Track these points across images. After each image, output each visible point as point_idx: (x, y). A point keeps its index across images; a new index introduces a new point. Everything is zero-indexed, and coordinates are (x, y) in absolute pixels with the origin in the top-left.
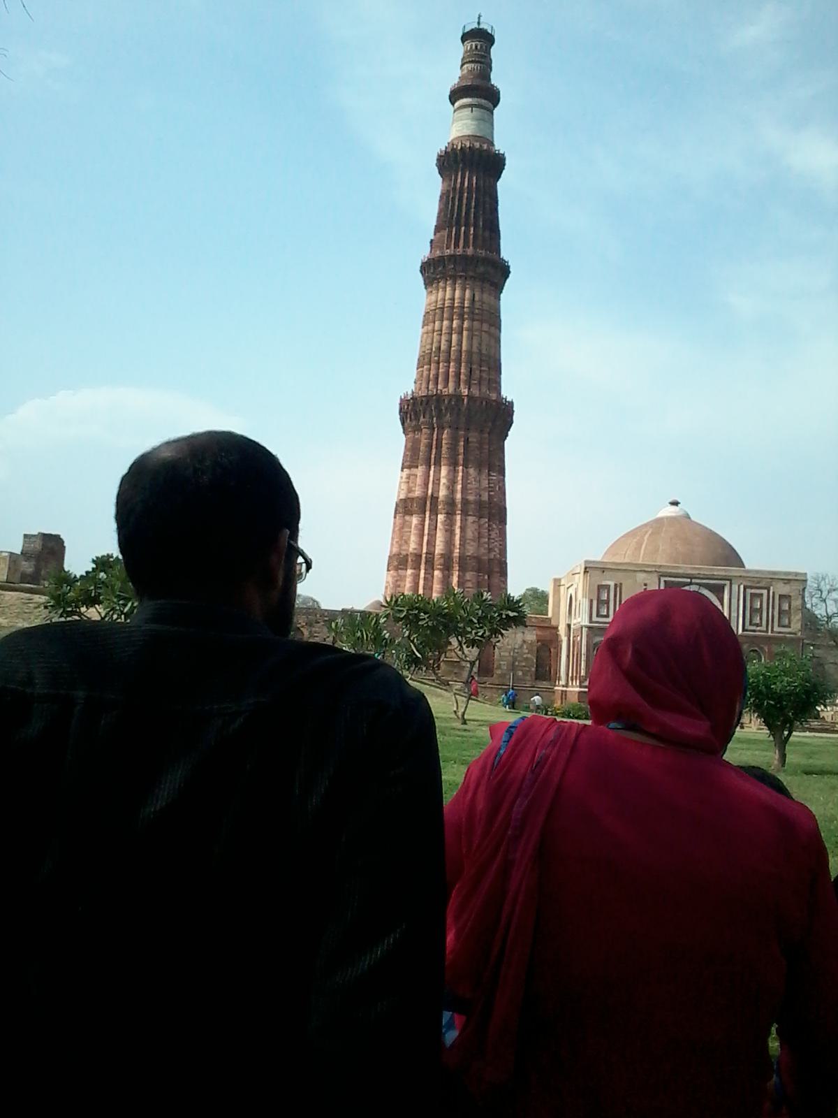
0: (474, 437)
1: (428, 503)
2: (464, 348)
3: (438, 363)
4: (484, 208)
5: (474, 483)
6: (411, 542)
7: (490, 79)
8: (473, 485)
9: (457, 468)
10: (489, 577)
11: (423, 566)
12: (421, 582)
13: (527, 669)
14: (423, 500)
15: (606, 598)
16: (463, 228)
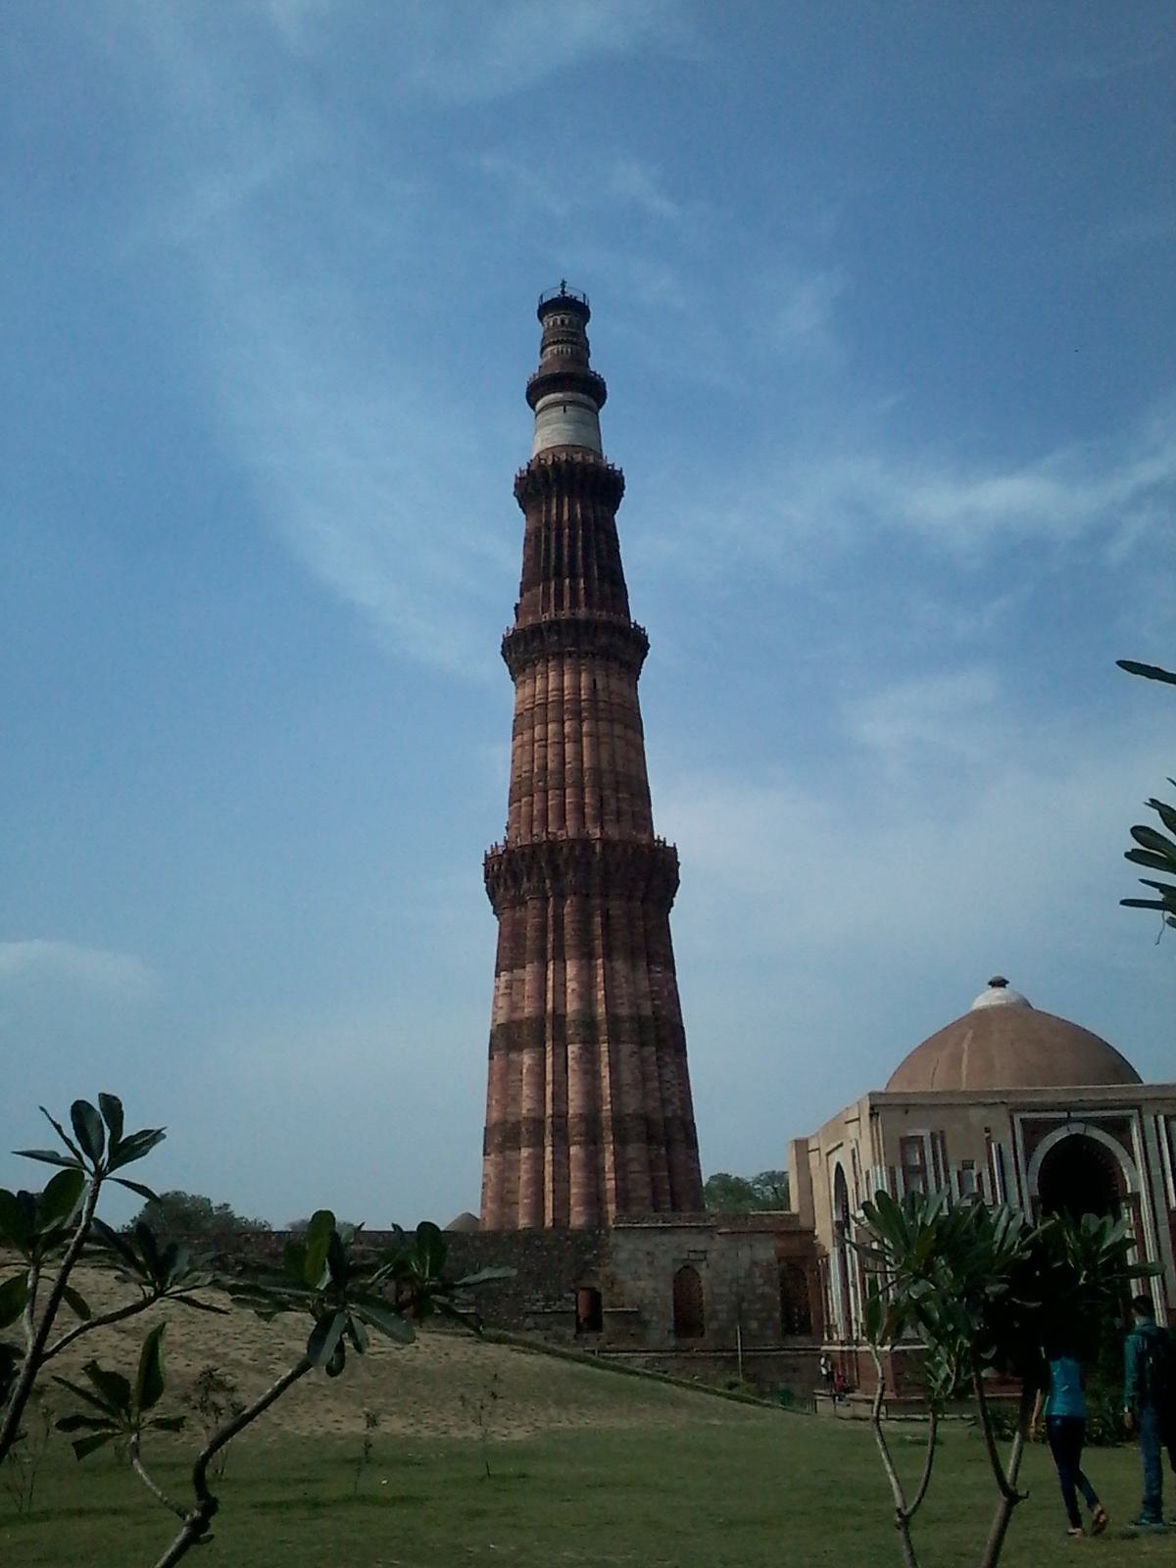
0: (616, 907)
1: (549, 1026)
2: (585, 766)
3: (546, 792)
4: (599, 552)
5: (624, 985)
6: (524, 1097)
7: (588, 366)
8: (623, 989)
9: (593, 963)
10: (667, 1150)
11: (548, 1141)
12: (549, 1170)
13: (764, 1315)
14: (539, 1021)
15: (918, 1163)
16: (567, 581)
